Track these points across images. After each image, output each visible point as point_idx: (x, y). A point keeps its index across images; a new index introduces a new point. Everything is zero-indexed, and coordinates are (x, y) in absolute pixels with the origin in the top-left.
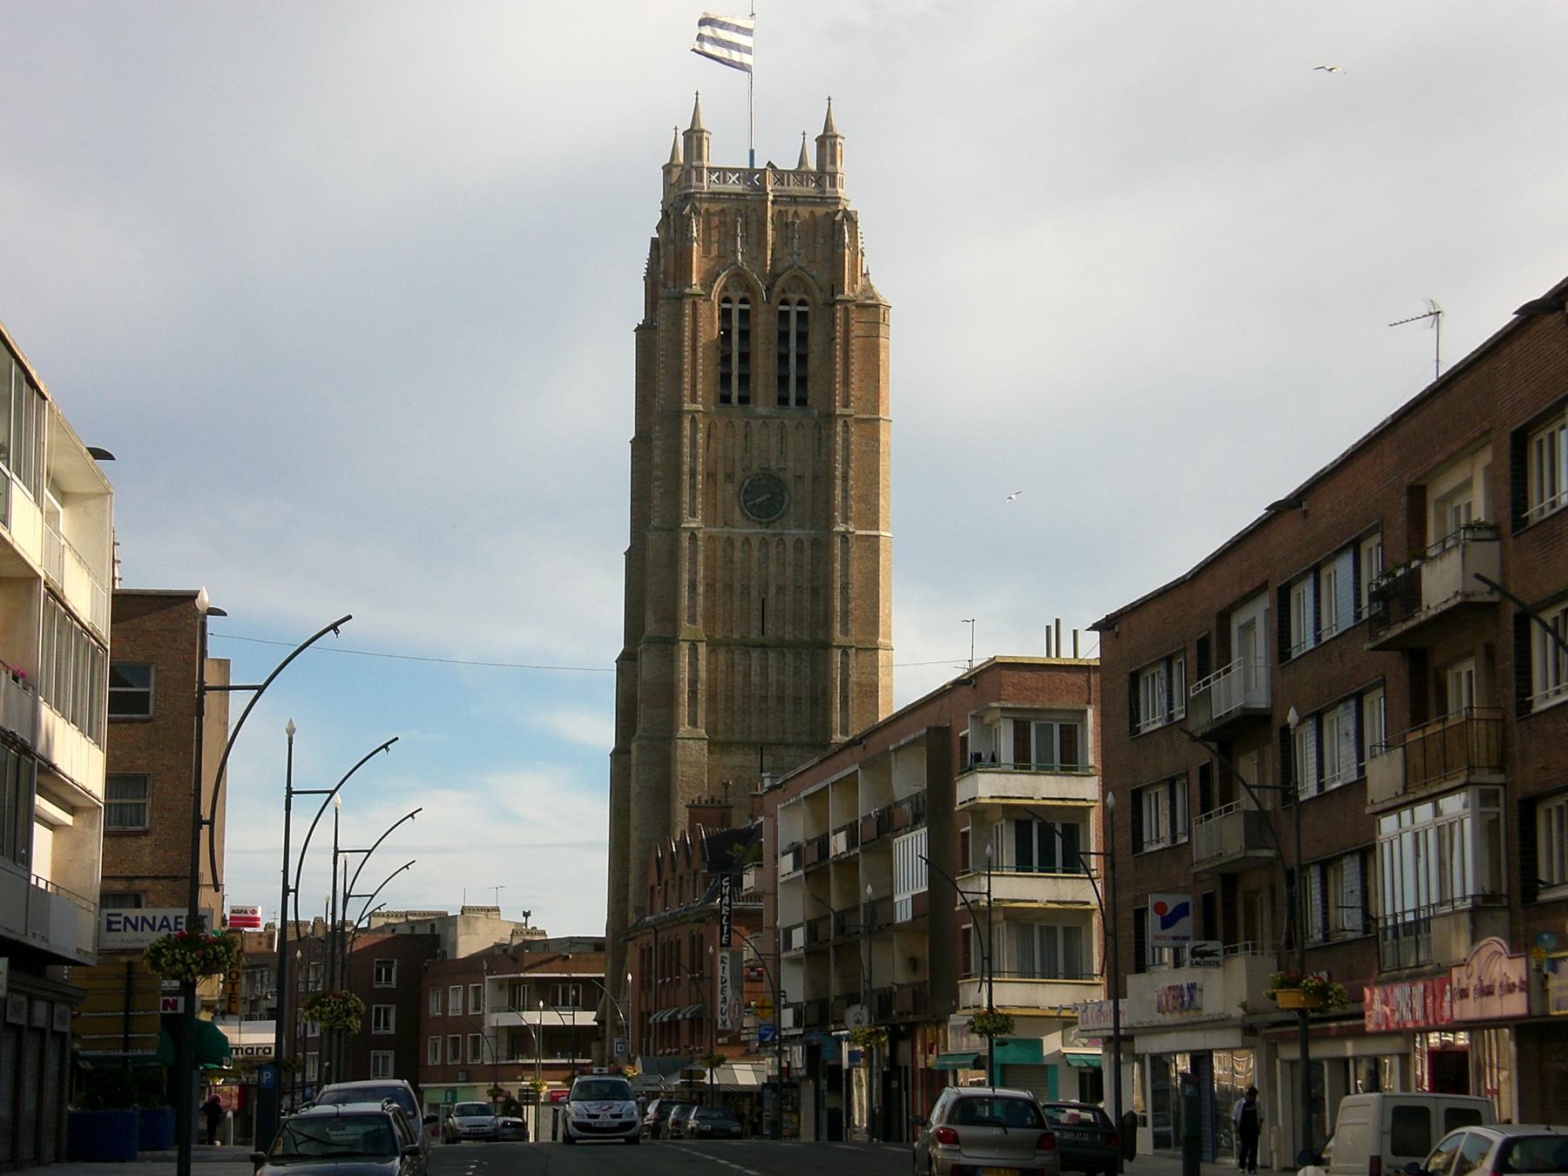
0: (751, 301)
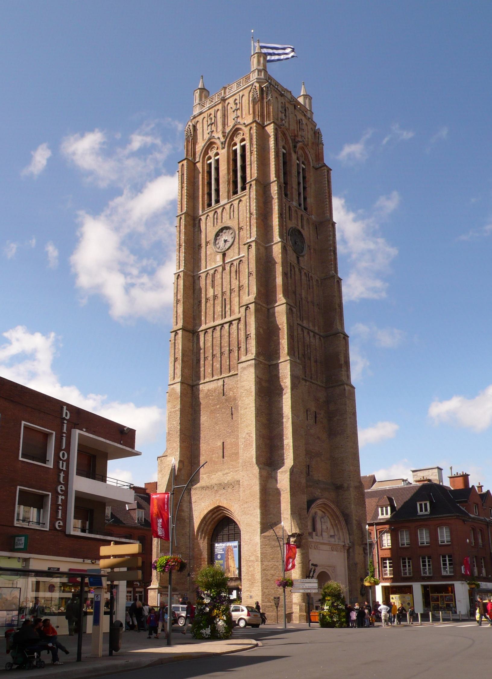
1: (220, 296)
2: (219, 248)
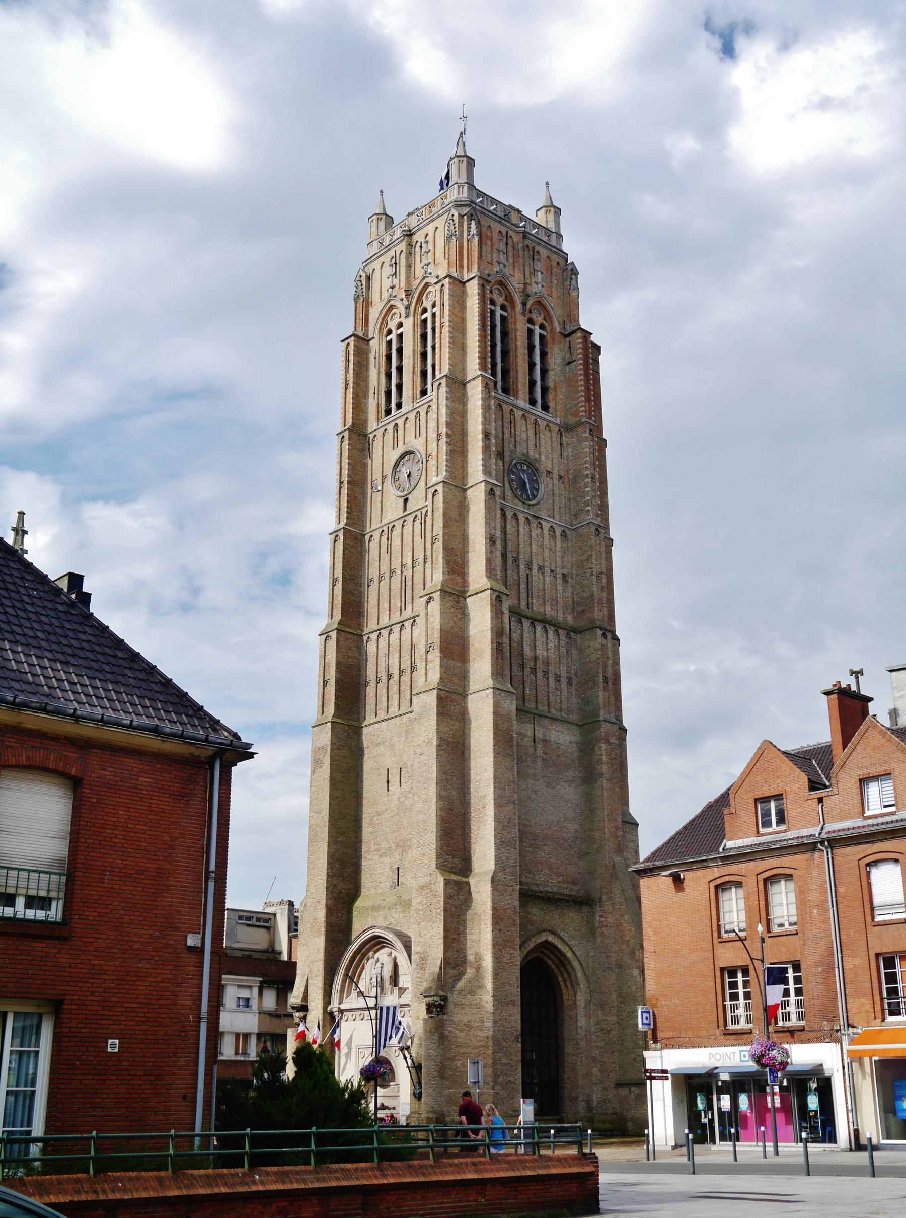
0: (509, 308)
1: (398, 572)
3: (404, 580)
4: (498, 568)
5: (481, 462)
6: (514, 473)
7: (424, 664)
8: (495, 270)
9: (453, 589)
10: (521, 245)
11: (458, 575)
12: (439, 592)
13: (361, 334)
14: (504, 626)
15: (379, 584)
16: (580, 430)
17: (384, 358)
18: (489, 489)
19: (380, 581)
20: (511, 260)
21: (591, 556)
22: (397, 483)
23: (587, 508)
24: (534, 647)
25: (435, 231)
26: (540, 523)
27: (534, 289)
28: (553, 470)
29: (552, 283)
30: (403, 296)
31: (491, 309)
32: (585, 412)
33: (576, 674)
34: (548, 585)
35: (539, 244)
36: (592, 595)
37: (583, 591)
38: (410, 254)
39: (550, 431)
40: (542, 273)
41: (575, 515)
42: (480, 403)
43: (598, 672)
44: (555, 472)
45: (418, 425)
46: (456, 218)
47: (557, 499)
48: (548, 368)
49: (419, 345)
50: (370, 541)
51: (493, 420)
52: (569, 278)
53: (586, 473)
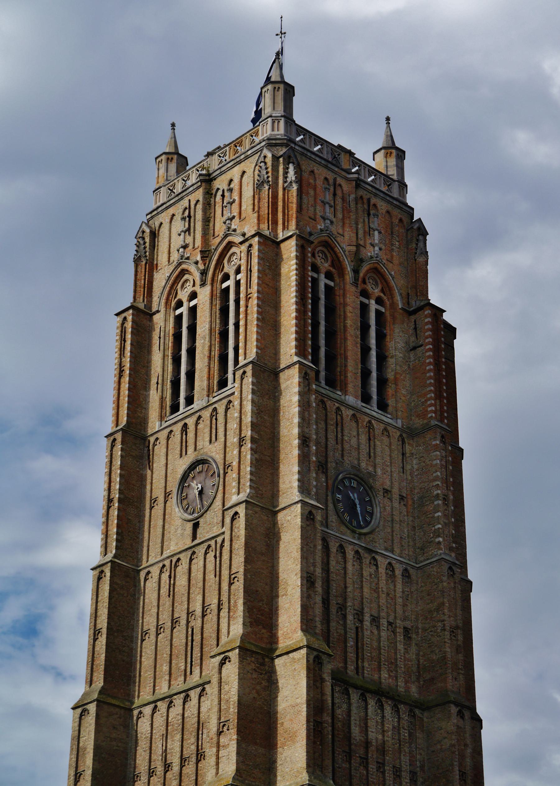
1: (183, 622)
2: (187, 509)
3: (190, 633)
4: (317, 619)
5: (296, 477)
6: (340, 492)
7: (215, 750)
8: (319, 227)
9: (256, 646)
10: (353, 196)
11: (264, 628)
12: (237, 651)
13: (141, 306)
14: (325, 698)
15: (157, 637)
16: (428, 436)
17: (171, 338)
18: (307, 512)
19: (157, 634)
20: (340, 216)
21: (443, 604)
22: (185, 502)
23: (437, 540)
24: (365, 729)
25: (242, 176)
26: (374, 559)
27: (369, 252)
28: (392, 488)
29: (392, 245)
30: (199, 258)
31: (312, 277)
32: (435, 412)
33: (422, 767)
34: (384, 643)
35: (376, 195)
36: (444, 658)
37: (432, 652)
38: (209, 204)
39: (389, 436)
40: (380, 233)
41: (422, 549)
42: (296, 398)
43: (452, 765)
44: (395, 490)
45: (214, 426)
46: (269, 160)
47: (397, 526)
48: (387, 354)
49: (218, 321)
50: (146, 580)
51: (313, 421)
52: (415, 240)
53: (435, 493)
